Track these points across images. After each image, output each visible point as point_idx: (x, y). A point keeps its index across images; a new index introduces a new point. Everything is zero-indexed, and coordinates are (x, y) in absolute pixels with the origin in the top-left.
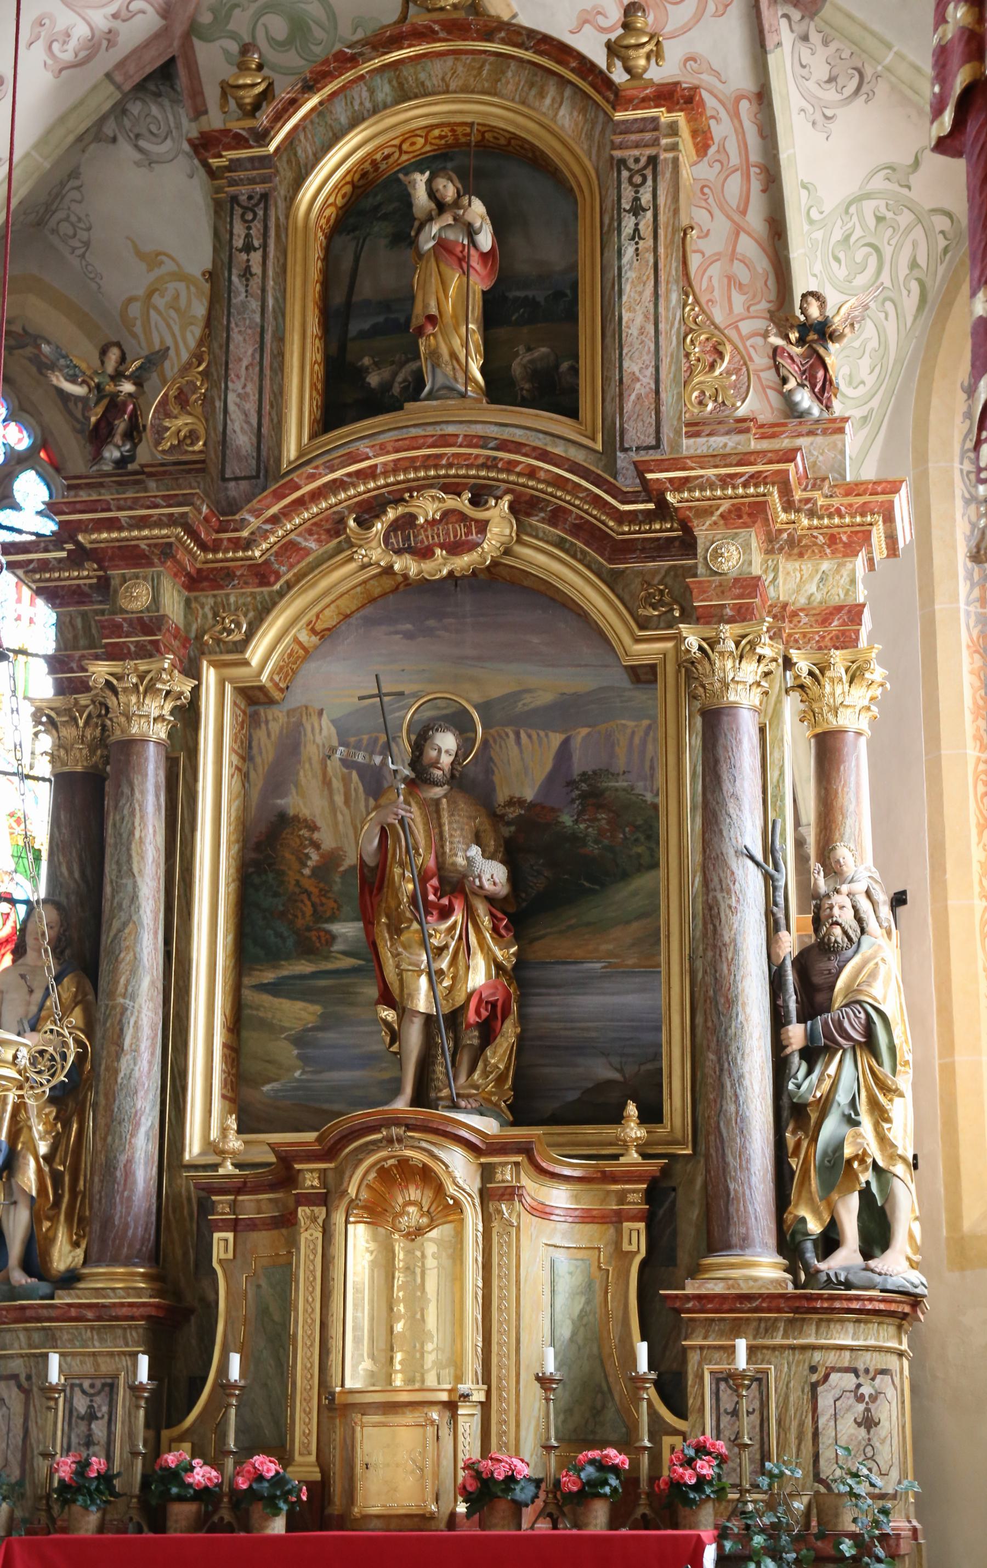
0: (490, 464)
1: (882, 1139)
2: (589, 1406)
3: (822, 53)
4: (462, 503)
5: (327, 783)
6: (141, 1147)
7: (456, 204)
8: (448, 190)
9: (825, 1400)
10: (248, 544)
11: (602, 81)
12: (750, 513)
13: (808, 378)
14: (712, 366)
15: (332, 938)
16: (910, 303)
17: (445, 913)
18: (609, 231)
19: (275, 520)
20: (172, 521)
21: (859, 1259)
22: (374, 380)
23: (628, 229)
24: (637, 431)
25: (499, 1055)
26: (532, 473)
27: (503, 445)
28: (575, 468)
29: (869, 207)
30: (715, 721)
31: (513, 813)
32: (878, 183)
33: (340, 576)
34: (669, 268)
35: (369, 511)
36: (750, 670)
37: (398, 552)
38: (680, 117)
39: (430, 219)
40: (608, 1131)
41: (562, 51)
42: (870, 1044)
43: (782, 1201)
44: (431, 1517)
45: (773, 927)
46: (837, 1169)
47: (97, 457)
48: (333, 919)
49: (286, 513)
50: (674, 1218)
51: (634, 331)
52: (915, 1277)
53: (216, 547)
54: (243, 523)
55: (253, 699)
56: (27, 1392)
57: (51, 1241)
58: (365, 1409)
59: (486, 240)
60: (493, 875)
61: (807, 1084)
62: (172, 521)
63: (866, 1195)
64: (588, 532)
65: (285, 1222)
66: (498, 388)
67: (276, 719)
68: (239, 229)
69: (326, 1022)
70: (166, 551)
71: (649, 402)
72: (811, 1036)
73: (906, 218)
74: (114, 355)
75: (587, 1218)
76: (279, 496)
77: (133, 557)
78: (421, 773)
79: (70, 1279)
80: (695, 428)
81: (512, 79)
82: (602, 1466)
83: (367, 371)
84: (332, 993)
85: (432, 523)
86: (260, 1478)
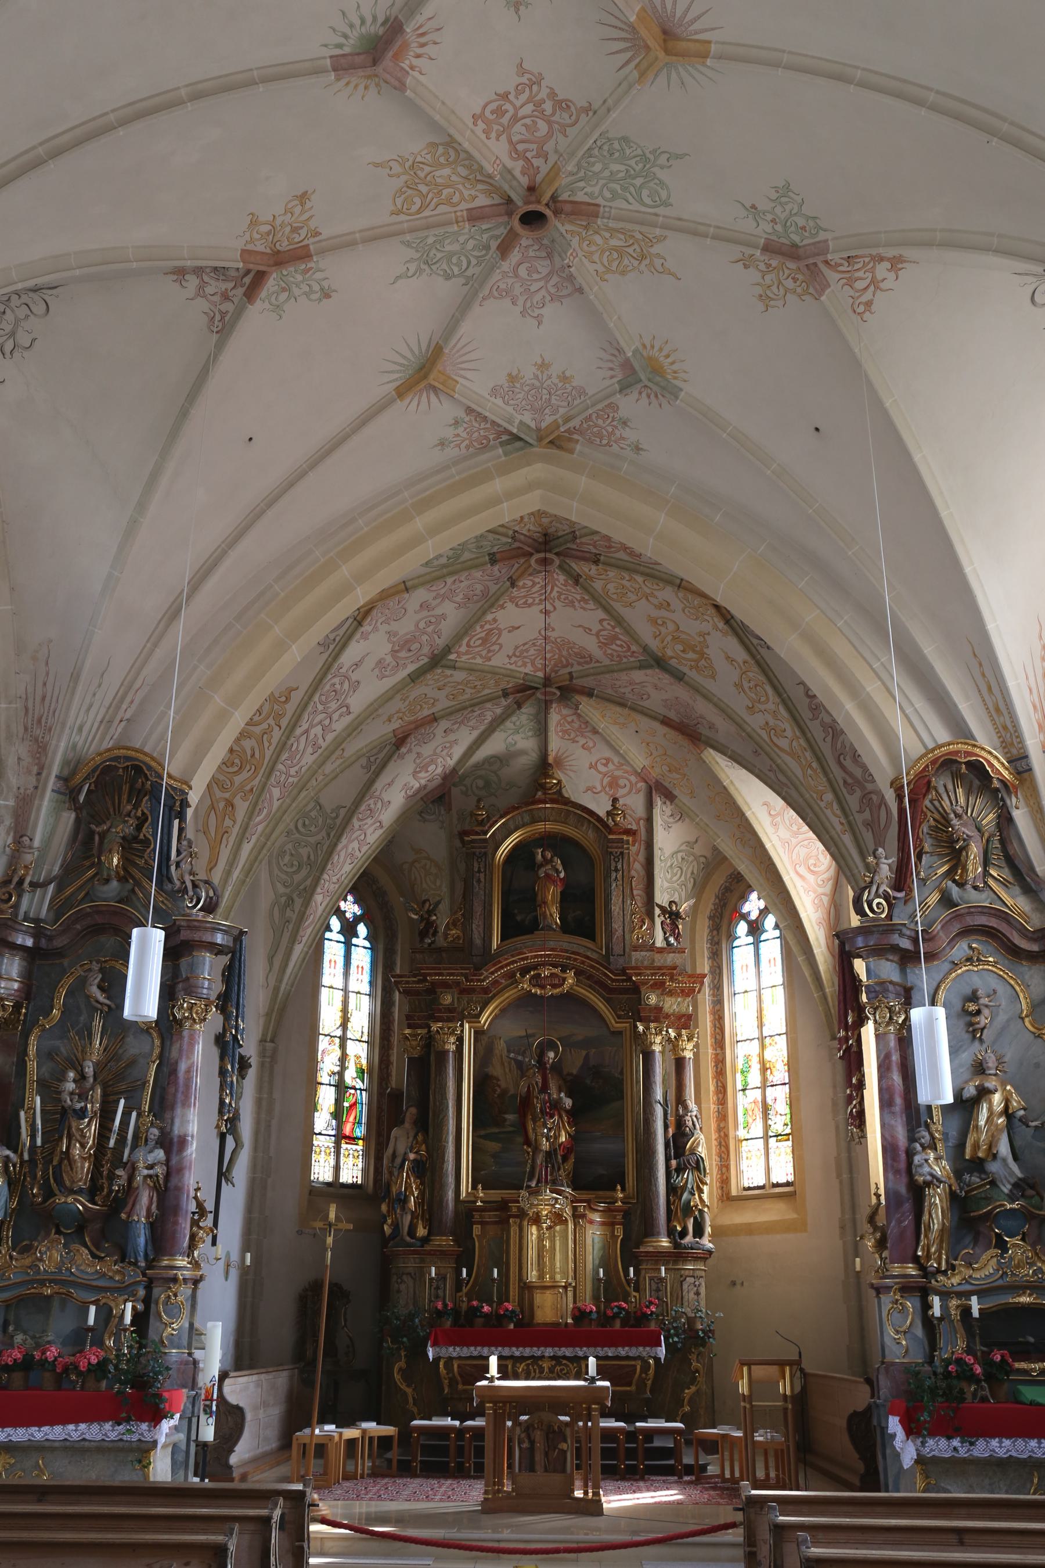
0: (569, 958)
1: (700, 1198)
2: (610, 1288)
3: (670, 807)
5: (503, 1064)
6: (451, 1194)
7: (551, 861)
8: (549, 855)
9: (685, 1286)
10: (483, 981)
12: (659, 986)
13: (673, 934)
14: (641, 927)
15: (505, 1120)
16: (690, 886)
17: (552, 1117)
18: (607, 876)
19: (492, 973)
20: (462, 974)
21: (692, 1239)
22: (519, 918)
23: (613, 877)
24: (617, 949)
25: (569, 1165)
26: (583, 963)
27: (573, 953)
28: (598, 963)
29: (680, 855)
30: (648, 1056)
31: (569, 1078)
32: (684, 847)
34: (628, 891)
35: (524, 971)
36: (658, 1039)
37: (534, 986)
38: (631, 839)
39: (541, 865)
40: (608, 1193)
43: (669, 1220)
44: (559, 1324)
45: (666, 1127)
46: (688, 1210)
47: (422, 940)
48: (505, 1113)
49: (496, 971)
50: (633, 1226)
51: (616, 913)
52: (711, 1245)
53: (472, 980)
54: (482, 974)
55: (478, 1034)
56: (414, 1279)
57: (416, 1228)
58: (537, 1288)
59: (562, 875)
60: (568, 1103)
61: (679, 1181)
62: (462, 974)
63: (695, 1219)
64: (602, 984)
65: (504, 1223)
67: (485, 1039)
68: (476, 865)
70: (458, 983)
71: (621, 939)
72: (678, 1164)
73: (691, 858)
74: (427, 905)
75: (603, 1224)
76: (494, 965)
77: (446, 985)
79: (425, 1240)
80: (636, 948)
82: (620, 1307)
85: (546, 977)
86: (507, 1310)
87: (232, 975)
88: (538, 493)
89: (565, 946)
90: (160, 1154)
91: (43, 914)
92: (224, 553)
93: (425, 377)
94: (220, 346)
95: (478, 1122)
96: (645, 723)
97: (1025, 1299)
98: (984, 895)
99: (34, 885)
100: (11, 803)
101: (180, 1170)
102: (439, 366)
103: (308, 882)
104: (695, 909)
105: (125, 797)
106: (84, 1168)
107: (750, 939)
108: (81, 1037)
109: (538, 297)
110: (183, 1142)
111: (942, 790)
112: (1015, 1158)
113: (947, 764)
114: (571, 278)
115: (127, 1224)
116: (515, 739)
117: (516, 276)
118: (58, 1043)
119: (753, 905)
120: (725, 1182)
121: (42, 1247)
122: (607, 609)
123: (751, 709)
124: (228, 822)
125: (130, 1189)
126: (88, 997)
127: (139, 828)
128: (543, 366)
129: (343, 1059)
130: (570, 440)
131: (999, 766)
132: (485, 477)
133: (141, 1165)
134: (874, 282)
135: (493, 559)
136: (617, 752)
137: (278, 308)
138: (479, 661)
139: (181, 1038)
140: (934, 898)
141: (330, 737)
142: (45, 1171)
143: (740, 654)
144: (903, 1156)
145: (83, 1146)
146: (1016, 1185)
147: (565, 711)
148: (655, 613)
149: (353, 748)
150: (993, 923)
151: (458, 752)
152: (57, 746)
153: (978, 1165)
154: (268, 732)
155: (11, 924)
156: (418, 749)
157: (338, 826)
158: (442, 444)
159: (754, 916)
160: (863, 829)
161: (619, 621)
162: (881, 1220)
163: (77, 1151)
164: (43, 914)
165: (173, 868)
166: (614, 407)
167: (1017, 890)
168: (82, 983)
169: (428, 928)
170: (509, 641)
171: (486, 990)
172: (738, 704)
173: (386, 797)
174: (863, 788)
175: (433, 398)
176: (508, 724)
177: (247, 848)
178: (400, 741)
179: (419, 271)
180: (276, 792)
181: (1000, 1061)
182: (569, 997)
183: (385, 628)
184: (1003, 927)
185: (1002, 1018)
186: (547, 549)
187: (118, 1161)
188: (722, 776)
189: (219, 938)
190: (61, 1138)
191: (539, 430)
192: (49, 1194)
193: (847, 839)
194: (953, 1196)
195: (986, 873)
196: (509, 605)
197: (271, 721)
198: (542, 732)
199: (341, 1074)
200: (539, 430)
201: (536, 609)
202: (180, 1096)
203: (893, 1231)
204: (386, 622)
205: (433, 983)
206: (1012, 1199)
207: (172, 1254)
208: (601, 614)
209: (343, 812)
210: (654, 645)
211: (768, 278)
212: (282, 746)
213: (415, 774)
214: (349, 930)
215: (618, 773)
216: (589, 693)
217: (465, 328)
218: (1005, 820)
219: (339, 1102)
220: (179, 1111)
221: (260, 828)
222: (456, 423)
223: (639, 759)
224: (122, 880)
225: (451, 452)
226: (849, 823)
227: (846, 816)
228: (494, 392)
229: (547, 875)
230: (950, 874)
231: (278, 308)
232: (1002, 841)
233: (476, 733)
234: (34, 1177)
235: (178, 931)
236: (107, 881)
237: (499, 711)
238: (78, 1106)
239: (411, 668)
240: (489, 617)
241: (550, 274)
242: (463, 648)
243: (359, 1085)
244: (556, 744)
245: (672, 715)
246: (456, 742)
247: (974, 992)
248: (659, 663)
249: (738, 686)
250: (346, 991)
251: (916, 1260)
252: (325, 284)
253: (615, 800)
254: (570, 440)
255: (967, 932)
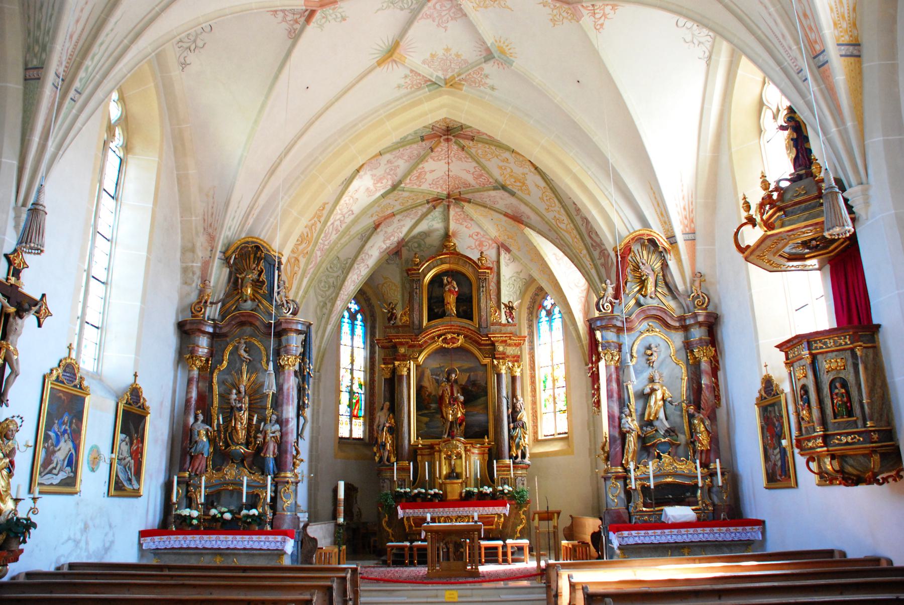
4: (455, 336)
6: (406, 442)
11: (477, 265)
16: (518, 293)
18: (478, 290)
24: (484, 325)
25: (462, 428)
30: (499, 376)
33: (434, 346)
35: (439, 336)
36: (504, 367)
41: (470, 259)
42: (523, 427)
43: (510, 451)
45: (508, 408)
50: (493, 454)
60: (462, 398)
61: (514, 433)
66: (459, 315)
69: (430, 421)
70: (407, 343)
77: (402, 344)
78: (448, 380)
80: (493, 324)
81: (461, 262)
83: (437, 311)
84: (431, 416)
87: (306, 344)
88: (445, 110)
89: (458, 324)
90: (277, 427)
91: (216, 317)
92: (296, 142)
93: (391, 56)
94: (293, 45)
95: (418, 408)
96: (496, 215)
97: (669, 480)
98: (654, 301)
99: (212, 303)
100: (199, 264)
101: (287, 434)
102: (398, 51)
103: (334, 295)
104: (521, 304)
105: (252, 260)
106: (242, 434)
107: (547, 319)
108: (238, 374)
109: (445, 18)
110: (287, 421)
111: (636, 252)
112: (667, 419)
113: (639, 239)
114: (461, 10)
115: (264, 458)
116: (433, 223)
117: (435, 8)
118: (227, 377)
119: (548, 303)
120: (536, 433)
121: (226, 469)
122: (477, 162)
123: (547, 210)
124: (296, 268)
125: (265, 443)
126: (240, 355)
127: (260, 275)
128: (448, 50)
129: (352, 379)
130: (460, 84)
131: (663, 242)
132: (419, 102)
133: (269, 431)
134: (604, 15)
135: (423, 139)
136: (482, 229)
137: (321, 26)
138: (415, 187)
139: (284, 373)
140: (633, 302)
141: (344, 226)
142: (225, 435)
143: (542, 184)
144: (617, 420)
145: (242, 424)
146: (666, 431)
147: (458, 210)
148: (501, 164)
149: (353, 231)
150: (659, 313)
151: (405, 230)
152: (219, 238)
153: (650, 423)
154: (314, 224)
155: (202, 322)
156: (385, 229)
157: (347, 268)
158: (399, 87)
159: (548, 308)
160: (601, 267)
161: (484, 168)
162: (607, 448)
163: (239, 426)
164: (216, 317)
165: (275, 294)
166: (482, 69)
167: (670, 298)
168: (236, 349)
169: (392, 316)
170: (430, 177)
171: (421, 346)
172: (542, 207)
173: (370, 253)
174: (600, 247)
175: (395, 65)
176: (429, 216)
177: (305, 281)
178: (377, 226)
179: (388, 7)
180: (319, 253)
181: (661, 376)
182: (461, 349)
183: (370, 173)
184: (663, 315)
185: (662, 356)
186: (449, 133)
187: (258, 430)
188: (533, 241)
189: (300, 327)
190: (231, 420)
191: (445, 79)
192: (227, 445)
193: (593, 272)
194: (639, 436)
195: (656, 291)
196: (430, 161)
197: (316, 219)
198: (446, 219)
199: (351, 387)
200: (445, 79)
201: (443, 162)
202: (285, 400)
203: (612, 453)
204: (371, 170)
205: (395, 343)
206: (664, 437)
207: (285, 472)
208: (475, 165)
209: (349, 261)
210: (501, 179)
211: (555, 11)
212: (321, 231)
213: (384, 241)
214: (353, 317)
215: (483, 239)
216: (469, 201)
217: (411, 33)
218: (665, 266)
219: (350, 400)
220: (285, 407)
221: (312, 270)
222: (406, 77)
223: (493, 232)
224: (253, 300)
225: (404, 91)
226: (594, 265)
227: (593, 261)
228: (424, 62)
229: (450, 290)
230: (639, 291)
231: (321, 26)
232: (664, 276)
233: (414, 221)
234: (220, 438)
235: (281, 324)
236: (246, 301)
237: (425, 210)
238: (239, 405)
239: (382, 191)
240: (421, 166)
241: (451, 8)
242: (408, 181)
243: (360, 391)
244: (453, 226)
245: (509, 212)
246: (404, 225)
247: (650, 345)
248: (504, 188)
249: (542, 199)
250: (352, 347)
251: (622, 465)
252: (343, 14)
253: (482, 253)
254: (460, 84)
255: (647, 318)
